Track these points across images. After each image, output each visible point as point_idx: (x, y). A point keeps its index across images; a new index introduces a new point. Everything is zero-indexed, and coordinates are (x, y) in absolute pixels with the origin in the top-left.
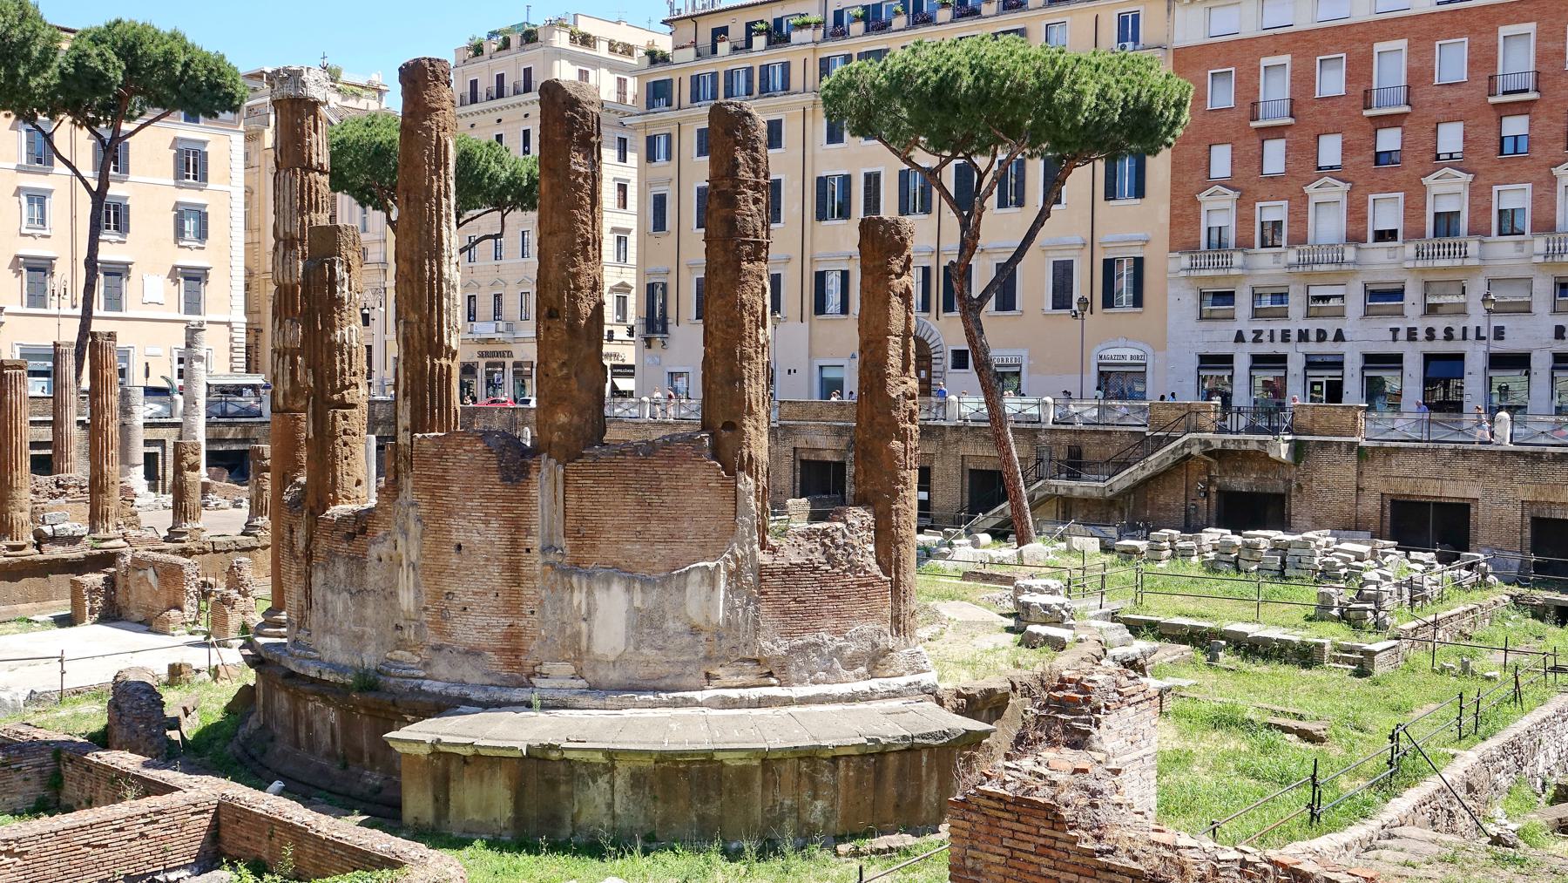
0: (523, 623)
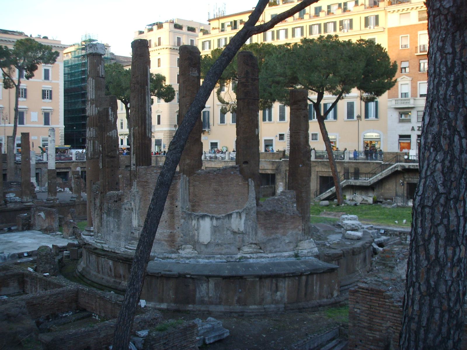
0: (175, 231)
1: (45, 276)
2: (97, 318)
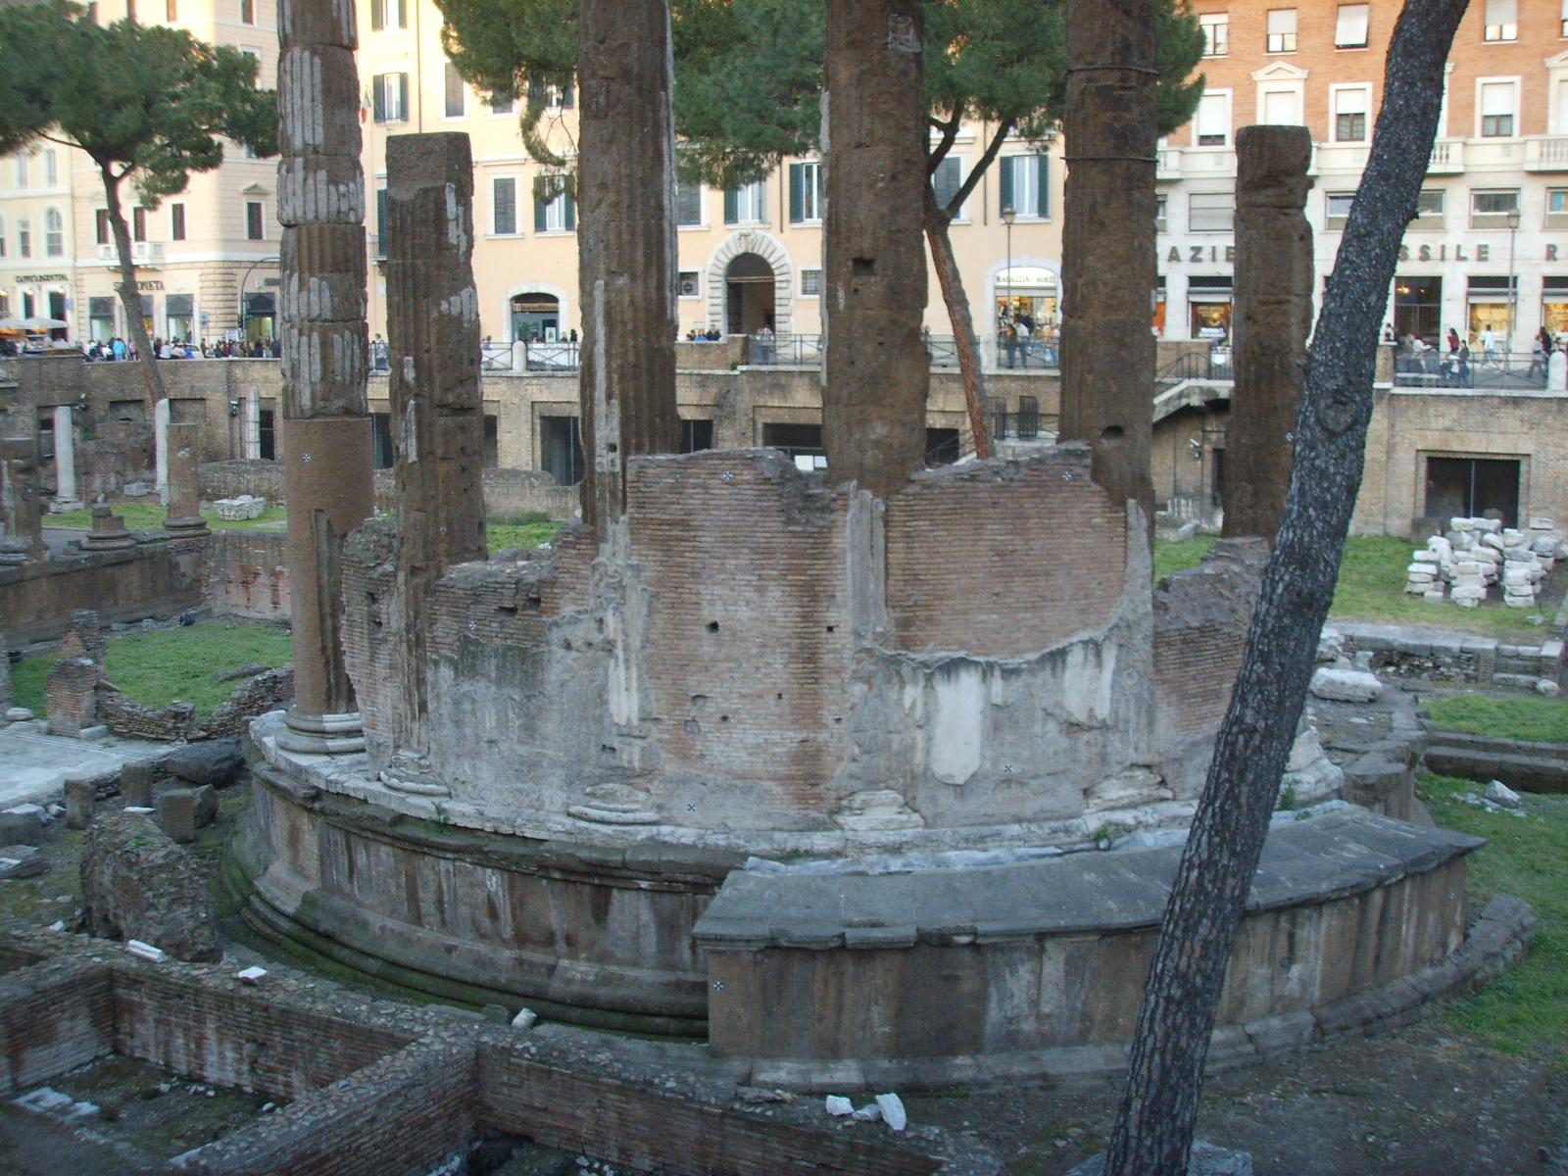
1: (247, 982)
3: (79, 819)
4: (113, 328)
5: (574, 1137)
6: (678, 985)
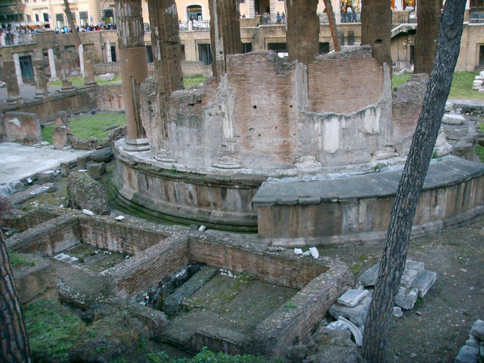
0: (290, 140)
1: (119, 221)
2: (230, 275)
3: (65, 174)
4: (63, 23)
5: (219, 263)
6: (248, 217)
